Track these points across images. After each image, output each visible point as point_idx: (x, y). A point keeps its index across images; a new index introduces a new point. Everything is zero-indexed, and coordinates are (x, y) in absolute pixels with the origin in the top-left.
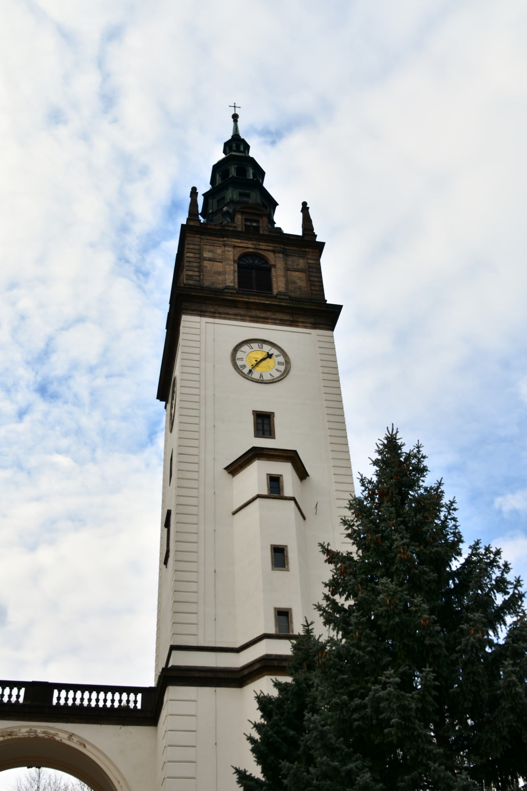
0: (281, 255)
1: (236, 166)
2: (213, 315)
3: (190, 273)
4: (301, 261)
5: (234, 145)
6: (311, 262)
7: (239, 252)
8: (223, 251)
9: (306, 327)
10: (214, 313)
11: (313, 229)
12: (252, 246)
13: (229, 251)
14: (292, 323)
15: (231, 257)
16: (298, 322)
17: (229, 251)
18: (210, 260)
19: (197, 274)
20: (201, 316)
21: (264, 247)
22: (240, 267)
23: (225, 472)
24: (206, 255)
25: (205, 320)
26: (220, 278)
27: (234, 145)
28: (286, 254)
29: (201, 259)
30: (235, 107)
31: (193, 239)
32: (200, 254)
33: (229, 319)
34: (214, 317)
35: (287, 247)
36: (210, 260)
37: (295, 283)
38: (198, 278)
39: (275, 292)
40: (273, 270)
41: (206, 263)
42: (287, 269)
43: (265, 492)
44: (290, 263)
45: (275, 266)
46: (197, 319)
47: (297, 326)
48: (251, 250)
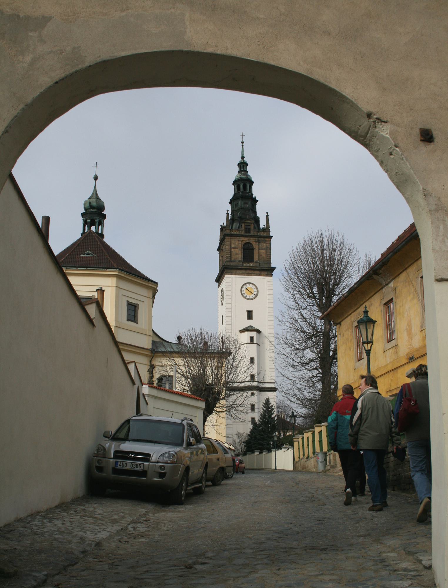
0: (257, 243)
1: (243, 184)
2: (235, 274)
3: (227, 256)
4: (264, 244)
5: (242, 166)
6: (268, 245)
7: (243, 242)
8: (238, 244)
9: (264, 276)
10: (235, 273)
11: (269, 228)
12: (248, 240)
13: (240, 244)
14: (260, 275)
15: (241, 246)
16: (261, 274)
17: (240, 244)
18: (234, 248)
19: (229, 256)
20: (231, 275)
21: (251, 240)
22: (244, 249)
23: (239, 332)
24: (233, 246)
25: (233, 276)
26: (237, 256)
27: (242, 166)
28: (259, 242)
29: (231, 248)
30: (242, 135)
31: (227, 239)
32: (231, 246)
33: (240, 275)
34: (235, 275)
35: (259, 239)
36: (234, 248)
37: (262, 255)
38: (230, 257)
39: (255, 260)
40: (254, 250)
41: (232, 250)
42: (259, 249)
43: (249, 342)
44: (260, 246)
45: (255, 248)
46: (229, 276)
47: (261, 276)
48: (247, 242)
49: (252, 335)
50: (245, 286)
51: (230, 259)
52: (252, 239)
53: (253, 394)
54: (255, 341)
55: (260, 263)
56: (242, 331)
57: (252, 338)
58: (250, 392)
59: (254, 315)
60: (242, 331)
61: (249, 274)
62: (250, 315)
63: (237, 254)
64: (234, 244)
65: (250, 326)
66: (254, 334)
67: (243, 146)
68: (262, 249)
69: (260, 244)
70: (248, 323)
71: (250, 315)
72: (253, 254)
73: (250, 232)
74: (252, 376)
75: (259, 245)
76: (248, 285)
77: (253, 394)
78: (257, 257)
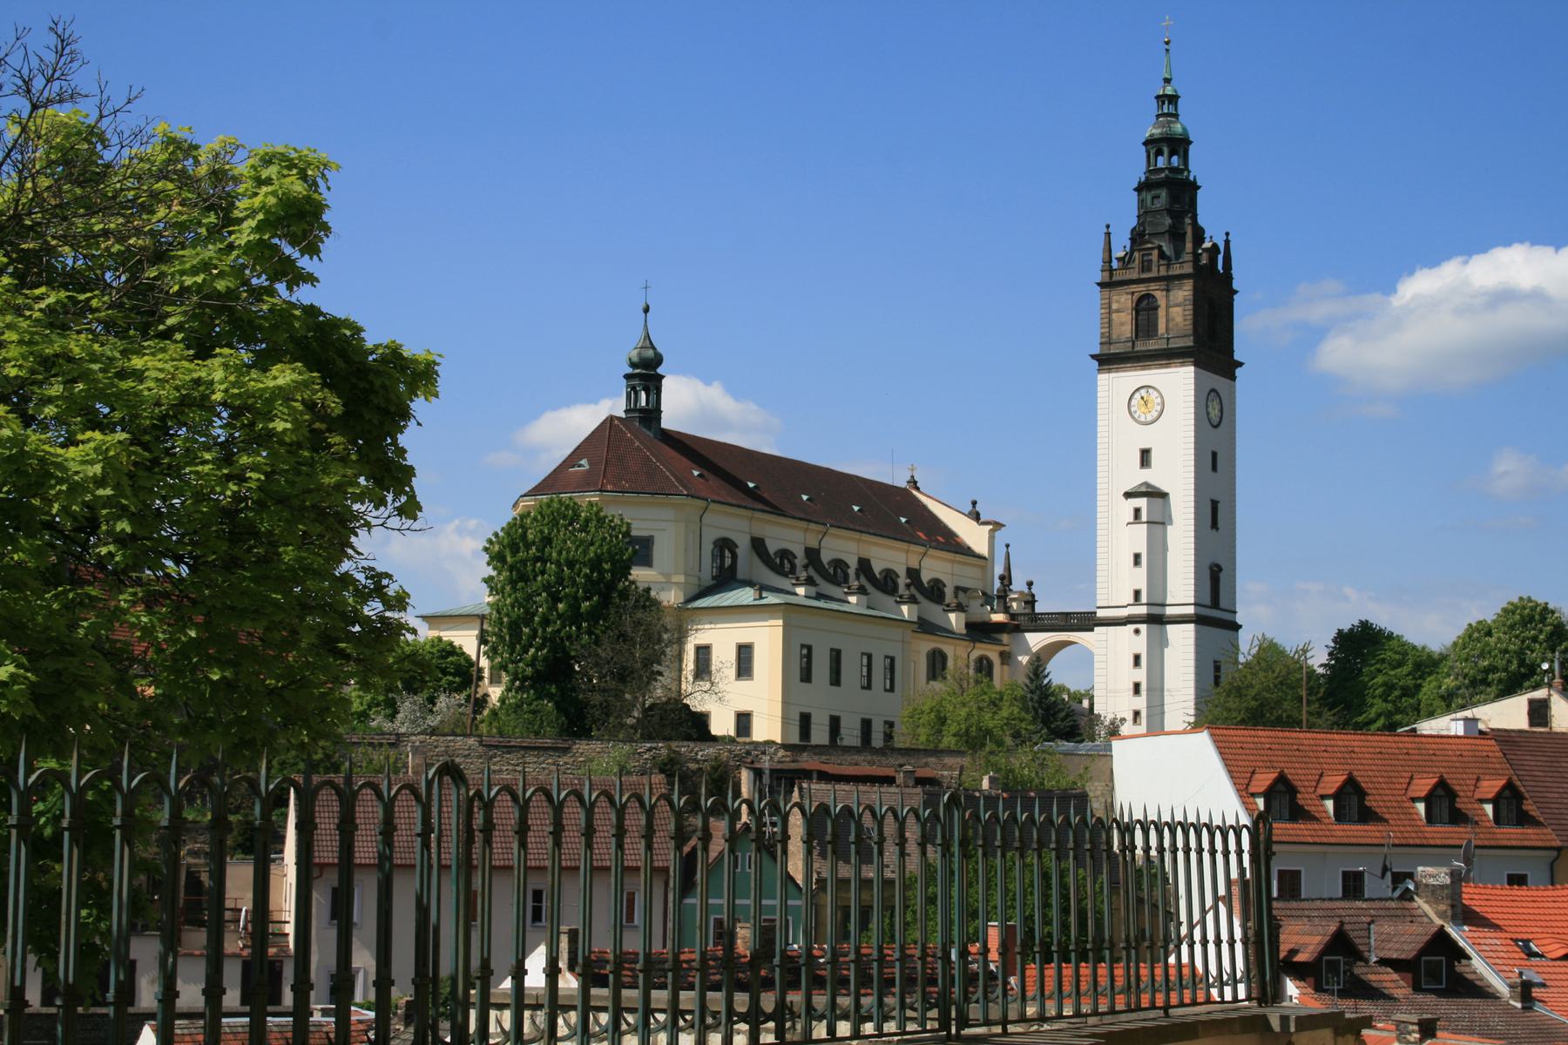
2: (1117, 370)
7: (1136, 296)
14: (1167, 366)
18: (1118, 311)
24: (1115, 306)
26: (1124, 328)
32: (1110, 307)
36: (1118, 311)
37: (1173, 320)
42: (1168, 307)
44: (1171, 298)
49: (1137, 506)
50: (1137, 396)
51: (1109, 337)
52: (1153, 286)
53: (1137, 631)
54: (1144, 518)
55: (1168, 339)
56: (1128, 495)
57: (1137, 511)
58: (1132, 627)
59: (1154, 456)
60: (1128, 495)
61: (1144, 368)
62: (1145, 457)
63: (1122, 324)
64: (1118, 302)
65: (1146, 484)
66: (1142, 503)
67: (1167, 50)
68: (1177, 305)
69: (1171, 293)
70: (1138, 477)
71: (1145, 457)
72: (1157, 319)
73: (1149, 270)
74: (1137, 594)
75: (1167, 297)
76: (1143, 392)
77: (1137, 631)
78: (1164, 326)
